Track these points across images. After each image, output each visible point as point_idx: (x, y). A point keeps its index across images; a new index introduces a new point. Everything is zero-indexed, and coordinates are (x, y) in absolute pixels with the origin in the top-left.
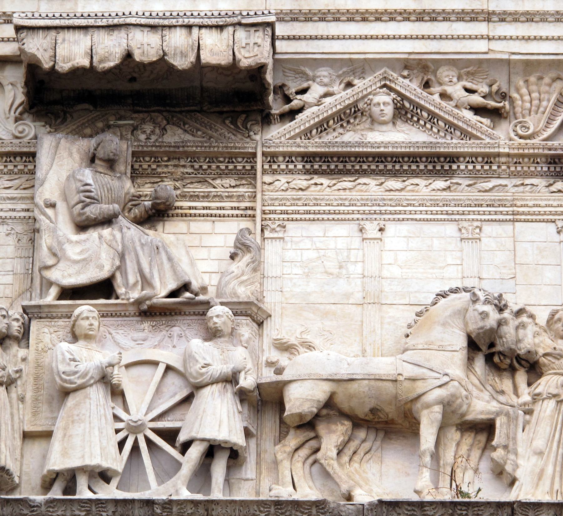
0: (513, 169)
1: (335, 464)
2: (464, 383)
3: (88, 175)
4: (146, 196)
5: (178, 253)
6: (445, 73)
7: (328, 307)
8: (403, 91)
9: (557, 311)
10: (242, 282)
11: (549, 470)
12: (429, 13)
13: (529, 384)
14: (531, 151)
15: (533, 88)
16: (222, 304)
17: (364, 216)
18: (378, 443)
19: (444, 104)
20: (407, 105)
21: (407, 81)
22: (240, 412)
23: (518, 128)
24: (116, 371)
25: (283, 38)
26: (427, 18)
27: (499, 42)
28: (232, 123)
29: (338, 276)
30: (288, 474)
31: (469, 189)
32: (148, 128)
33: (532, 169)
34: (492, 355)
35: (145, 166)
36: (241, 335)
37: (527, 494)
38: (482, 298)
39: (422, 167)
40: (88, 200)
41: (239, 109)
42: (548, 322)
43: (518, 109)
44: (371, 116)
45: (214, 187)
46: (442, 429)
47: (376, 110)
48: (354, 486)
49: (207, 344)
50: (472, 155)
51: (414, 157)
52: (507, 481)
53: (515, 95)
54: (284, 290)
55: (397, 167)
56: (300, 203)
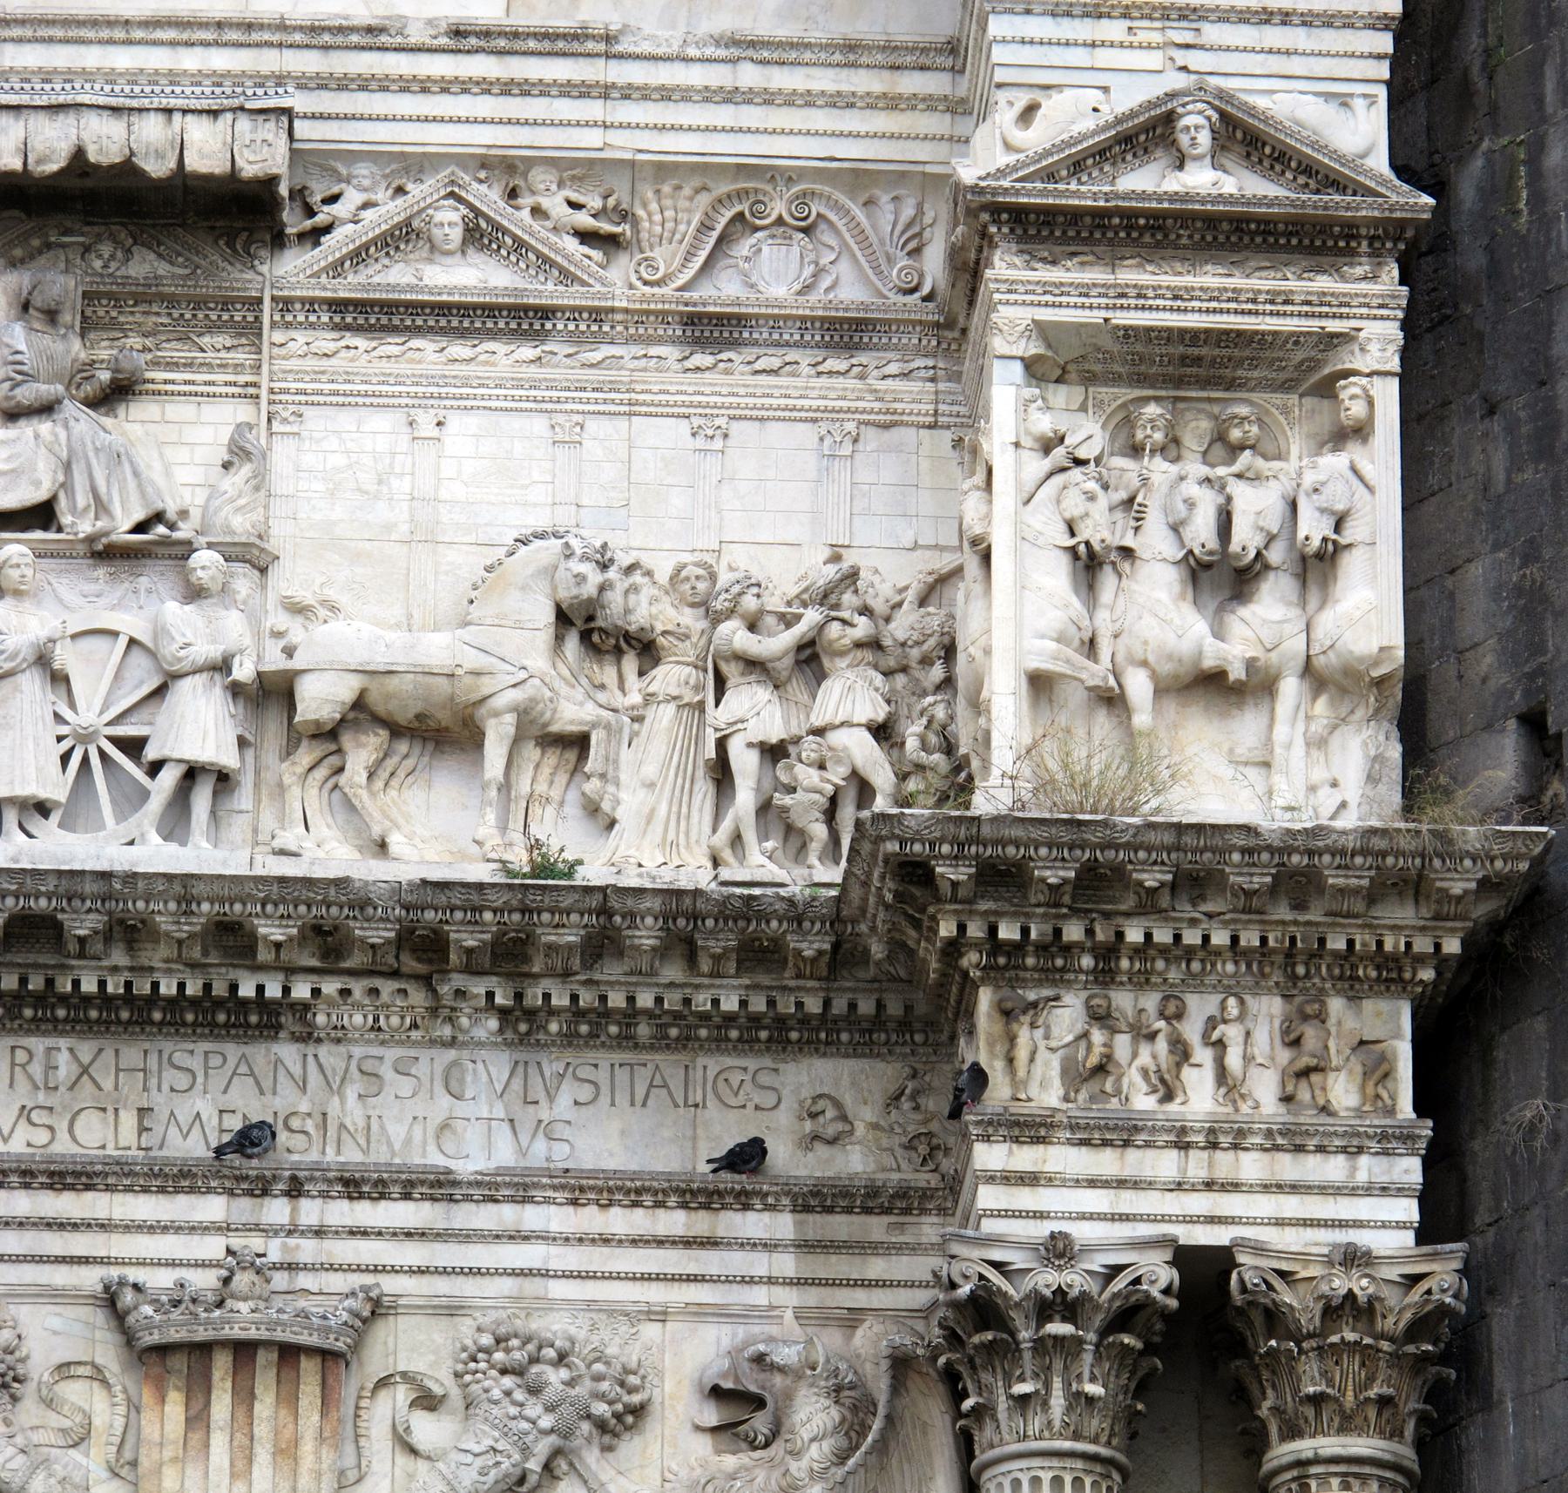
0: (632, 331)
1: (364, 794)
2: (547, 680)
3: (18, 337)
4: (102, 361)
5: (147, 458)
6: (541, 178)
7: (361, 544)
8: (478, 204)
9: (685, 566)
10: (238, 509)
11: (663, 809)
12: (519, 84)
13: (641, 674)
14: (660, 306)
15: (668, 202)
16: (210, 546)
17: (416, 402)
18: (426, 759)
19: (536, 226)
20: (483, 224)
21: (483, 188)
22: (232, 716)
23: (642, 269)
24: (58, 651)
25: (305, 116)
26: (516, 91)
27: (620, 131)
28: (227, 244)
29: (376, 497)
30: (298, 806)
31: (568, 361)
32: (106, 249)
33: (661, 332)
34: (591, 630)
35: (101, 313)
36: (235, 592)
37: (629, 847)
38: (579, 552)
39: (501, 325)
40: (19, 377)
41: (239, 224)
42: (671, 579)
43: (644, 235)
44: (430, 240)
45: (203, 351)
46: (517, 741)
47: (437, 233)
48: (390, 829)
49: (187, 608)
50: (573, 309)
51: (490, 310)
52: (604, 822)
53: (641, 213)
54: (301, 515)
55: (466, 324)
56: (324, 378)
